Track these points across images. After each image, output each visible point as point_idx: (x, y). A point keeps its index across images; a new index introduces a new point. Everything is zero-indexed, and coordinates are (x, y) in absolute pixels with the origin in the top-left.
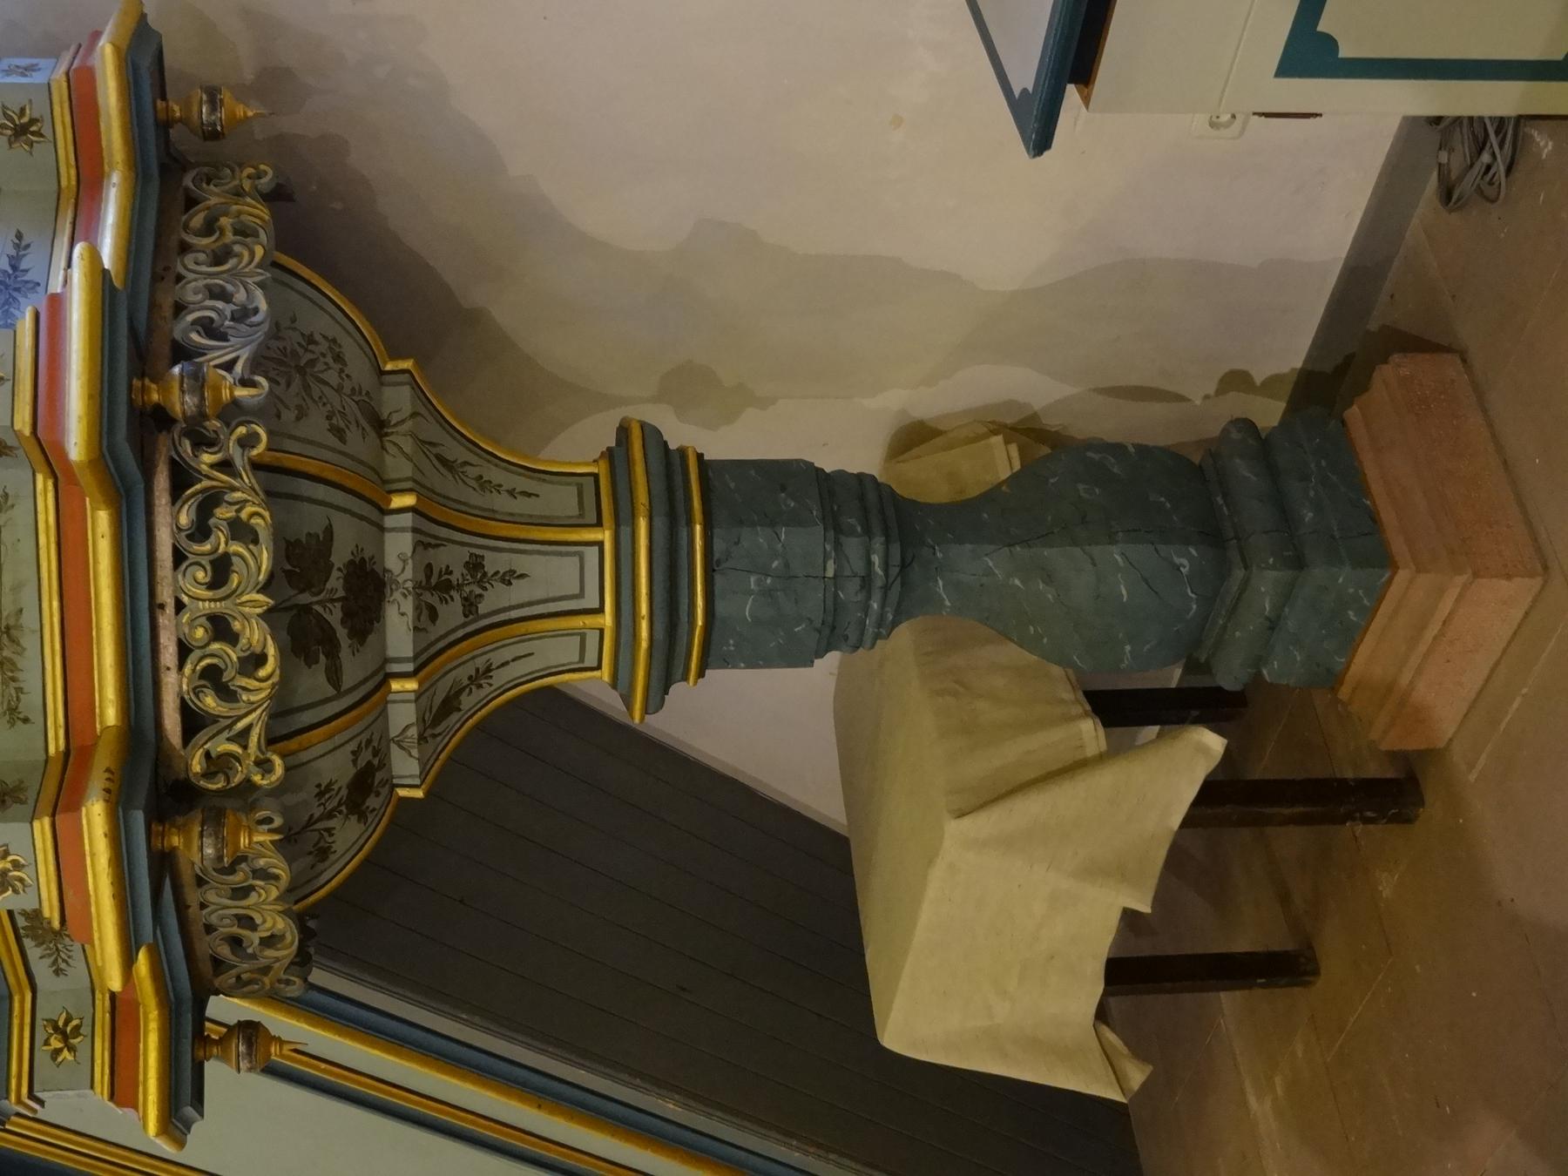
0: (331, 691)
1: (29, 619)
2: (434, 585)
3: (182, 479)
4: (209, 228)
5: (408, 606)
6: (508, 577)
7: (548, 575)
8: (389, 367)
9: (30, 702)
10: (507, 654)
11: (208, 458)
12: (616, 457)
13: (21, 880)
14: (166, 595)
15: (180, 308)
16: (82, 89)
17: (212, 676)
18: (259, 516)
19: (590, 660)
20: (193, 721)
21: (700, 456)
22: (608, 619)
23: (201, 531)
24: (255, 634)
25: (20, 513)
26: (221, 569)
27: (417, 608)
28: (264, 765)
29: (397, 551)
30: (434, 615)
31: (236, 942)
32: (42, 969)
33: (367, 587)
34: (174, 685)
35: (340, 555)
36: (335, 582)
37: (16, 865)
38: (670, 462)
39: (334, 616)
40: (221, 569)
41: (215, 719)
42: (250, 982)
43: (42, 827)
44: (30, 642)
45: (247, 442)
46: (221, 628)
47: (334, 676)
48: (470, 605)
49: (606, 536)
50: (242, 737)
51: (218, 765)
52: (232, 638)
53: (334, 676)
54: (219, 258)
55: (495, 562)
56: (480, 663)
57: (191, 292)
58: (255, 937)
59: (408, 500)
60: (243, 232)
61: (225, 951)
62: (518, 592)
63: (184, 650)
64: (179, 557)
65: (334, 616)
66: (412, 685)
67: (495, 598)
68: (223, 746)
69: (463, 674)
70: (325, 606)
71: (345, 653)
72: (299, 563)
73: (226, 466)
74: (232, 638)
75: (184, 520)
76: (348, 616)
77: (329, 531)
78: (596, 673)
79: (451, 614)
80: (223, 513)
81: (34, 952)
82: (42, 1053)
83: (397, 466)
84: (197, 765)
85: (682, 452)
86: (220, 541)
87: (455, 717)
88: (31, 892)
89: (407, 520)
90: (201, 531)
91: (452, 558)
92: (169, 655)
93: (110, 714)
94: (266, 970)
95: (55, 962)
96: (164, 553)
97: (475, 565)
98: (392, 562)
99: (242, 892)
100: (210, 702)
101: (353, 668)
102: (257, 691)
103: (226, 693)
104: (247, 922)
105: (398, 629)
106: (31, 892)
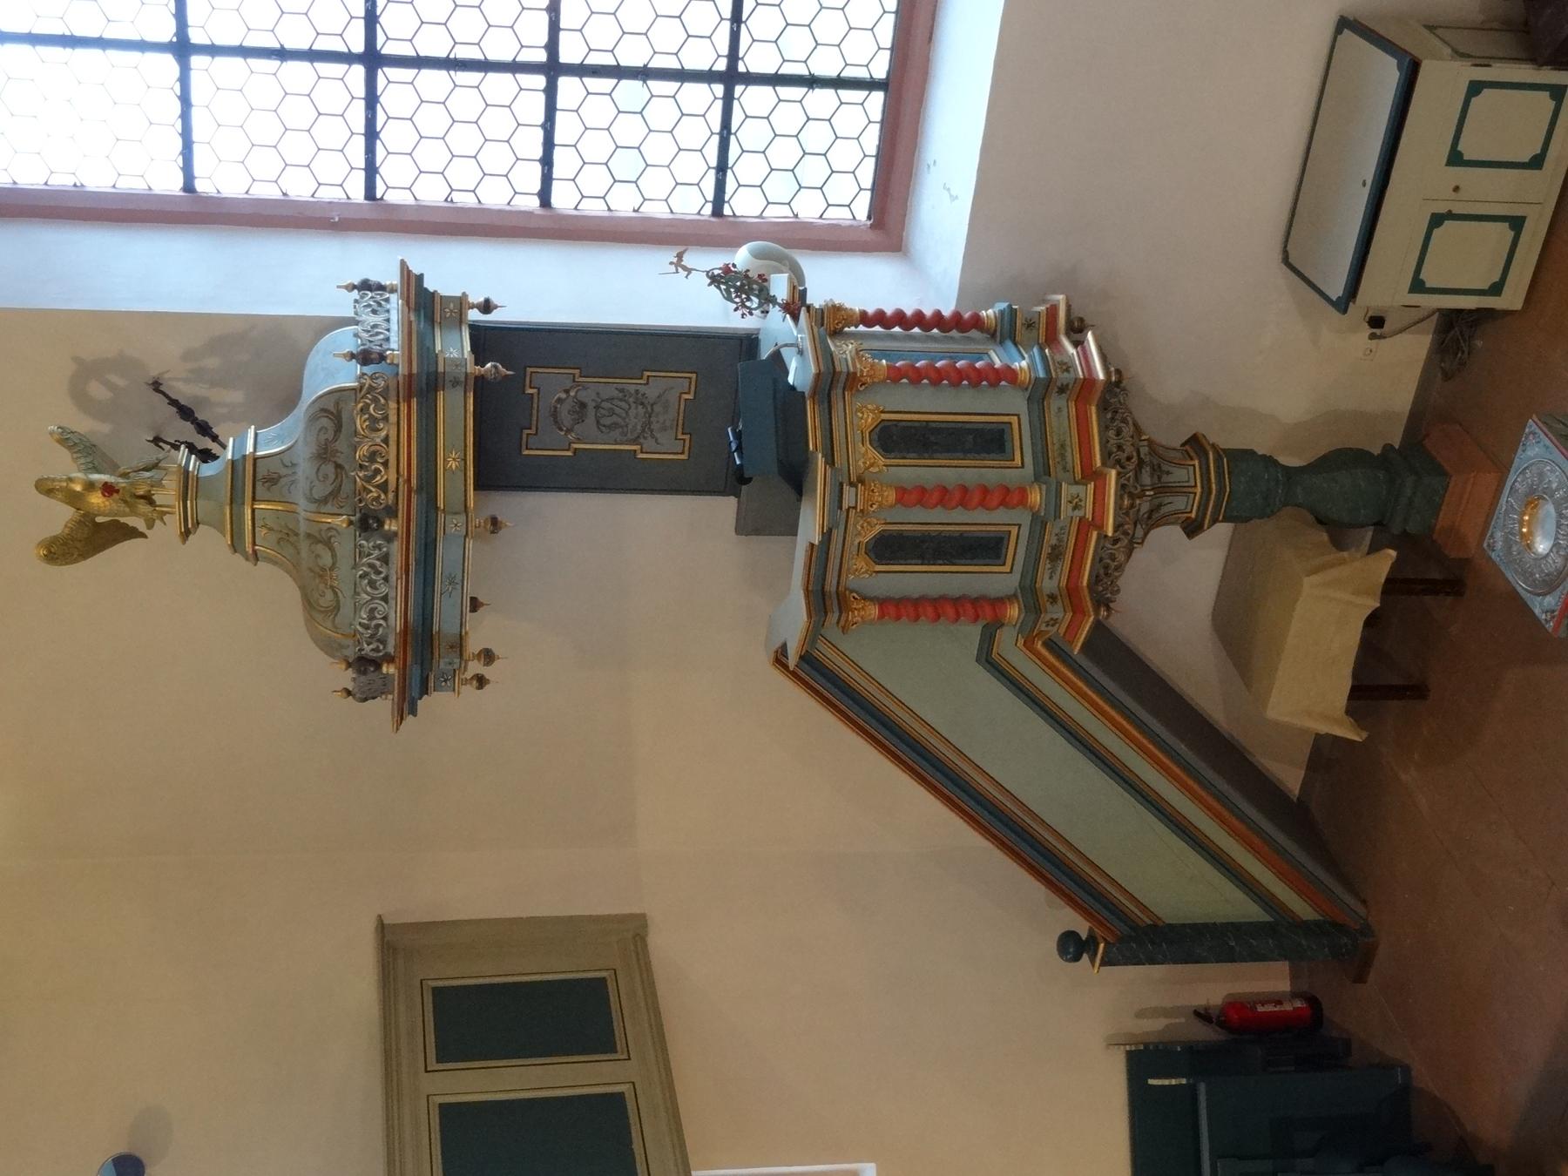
6: (1168, 473)
9: (1069, 466)
10: (1167, 500)
22: (1199, 490)
24: (1129, 449)
43: (1091, 486)
46: (1120, 447)
49: (1196, 463)
55: (1165, 467)
58: (1113, 564)
67: (1165, 478)
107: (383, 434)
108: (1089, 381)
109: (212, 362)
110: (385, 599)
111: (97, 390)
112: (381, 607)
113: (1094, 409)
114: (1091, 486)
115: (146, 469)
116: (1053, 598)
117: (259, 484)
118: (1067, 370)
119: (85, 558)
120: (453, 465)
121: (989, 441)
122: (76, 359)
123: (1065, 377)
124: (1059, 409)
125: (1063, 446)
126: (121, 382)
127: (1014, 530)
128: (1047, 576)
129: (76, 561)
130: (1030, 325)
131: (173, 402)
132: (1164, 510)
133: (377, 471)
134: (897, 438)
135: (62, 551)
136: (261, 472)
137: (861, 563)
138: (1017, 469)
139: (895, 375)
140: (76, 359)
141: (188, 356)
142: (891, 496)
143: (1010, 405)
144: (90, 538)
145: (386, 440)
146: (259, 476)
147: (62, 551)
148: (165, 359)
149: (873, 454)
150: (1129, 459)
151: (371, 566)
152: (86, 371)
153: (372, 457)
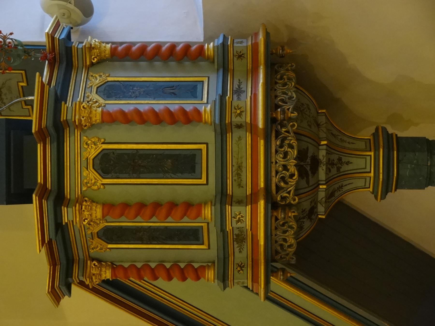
0: (307, 186)
1: (244, 165)
2: (330, 164)
3: (278, 134)
4: (281, 78)
5: (324, 168)
6: (348, 163)
7: (357, 163)
8: (320, 112)
9: (243, 183)
11: (284, 130)
12: (375, 135)
13: (243, 220)
14: (273, 160)
15: (276, 97)
16: (255, 47)
17: (283, 179)
18: (294, 142)
19: (367, 186)
20: (278, 188)
21: (396, 135)
22: (372, 174)
23: (281, 146)
24: (293, 169)
25: (243, 141)
26: (286, 154)
27: (326, 169)
28: (294, 200)
29: (322, 154)
30: (330, 171)
31: (281, 245)
32: (237, 250)
33: (315, 163)
34: (275, 180)
35: (310, 154)
36: (309, 160)
37: (242, 217)
38: (389, 137)
39: (308, 168)
40: (286, 154)
41: (283, 188)
42: (284, 258)
43: (249, 208)
44: (244, 170)
45: (293, 126)
46: (285, 168)
47: (308, 182)
48: (338, 169)
49: (372, 154)
50: (289, 193)
51: (283, 198)
52: (288, 170)
53: (308, 182)
54: (285, 85)
55: (344, 159)
56: (340, 184)
57: (279, 93)
58: (286, 245)
59: (325, 142)
60: (289, 79)
61: (279, 248)
62: (350, 167)
63: (277, 172)
64: (276, 152)
65: (308, 168)
66: (325, 187)
67: (345, 168)
68: (285, 194)
69: (336, 186)
70: (307, 165)
71: (310, 177)
72: (302, 156)
73: (288, 132)
74: (288, 170)
75: (278, 143)
76: (311, 169)
77: (308, 148)
78: (369, 189)
79: (334, 171)
80: (287, 142)
81: (236, 246)
82: (236, 272)
83: (322, 135)
84: (279, 199)
85: (392, 134)
86: (286, 148)
87: (333, 198)
88: (245, 223)
89: (325, 147)
90: (281, 146)
91: (335, 157)
92: (274, 174)
93: (262, 185)
94: (287, 255)
95: (240, 249)
96: (273, 150)
97: (340, 159)
98: (321, 157)
99: (285, 232)
100: (282, 184)
101: (312, 181)
102: (292, 182)
103: (286, 183)
104: (285, 240)
105: (322, 174)
106: (245, 223)
108: (253, 127)
113: (262, 142)
114: (249, 208)
116: (241, 266)
118: (240, 115)
121: (184, 164)
123: (236, 120)
124: (240, 138)
125: (240, 167)
127: (205, 225)
128: (237, 250)
130: (240, 56)
132: (345, 189)
134: (111, 164)
137: (97, 242)
138: (199, 187)
139: (109, 119)
142: (98, 212)
143: (199, 139)
149: (92, 175)
150: (292, 176)
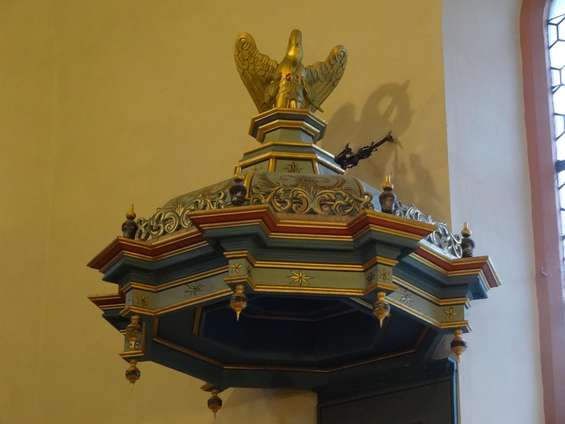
107: (318, 210)
109: (411, 177)
110: (179, 228)
111: (385, 103)
112: (173, 226)
115: (305, 93)
117: (290, 162)
119: (243, 75)
120: (296, 278)
122: (407, 84)
126: (392, 118)
129: (238, 66)
131: (374, 147)
133: (283, 203)
135: (245, 51)
136: (300, 164)
140: (407, 84)
141: (414, 159)
144: (259, 80)
145: (312, 212)
146: (296, 162)
147: (245, 51)
148: (411, 143)
151: (205, 207)
152: (398, 92)
153: (298, 201)
